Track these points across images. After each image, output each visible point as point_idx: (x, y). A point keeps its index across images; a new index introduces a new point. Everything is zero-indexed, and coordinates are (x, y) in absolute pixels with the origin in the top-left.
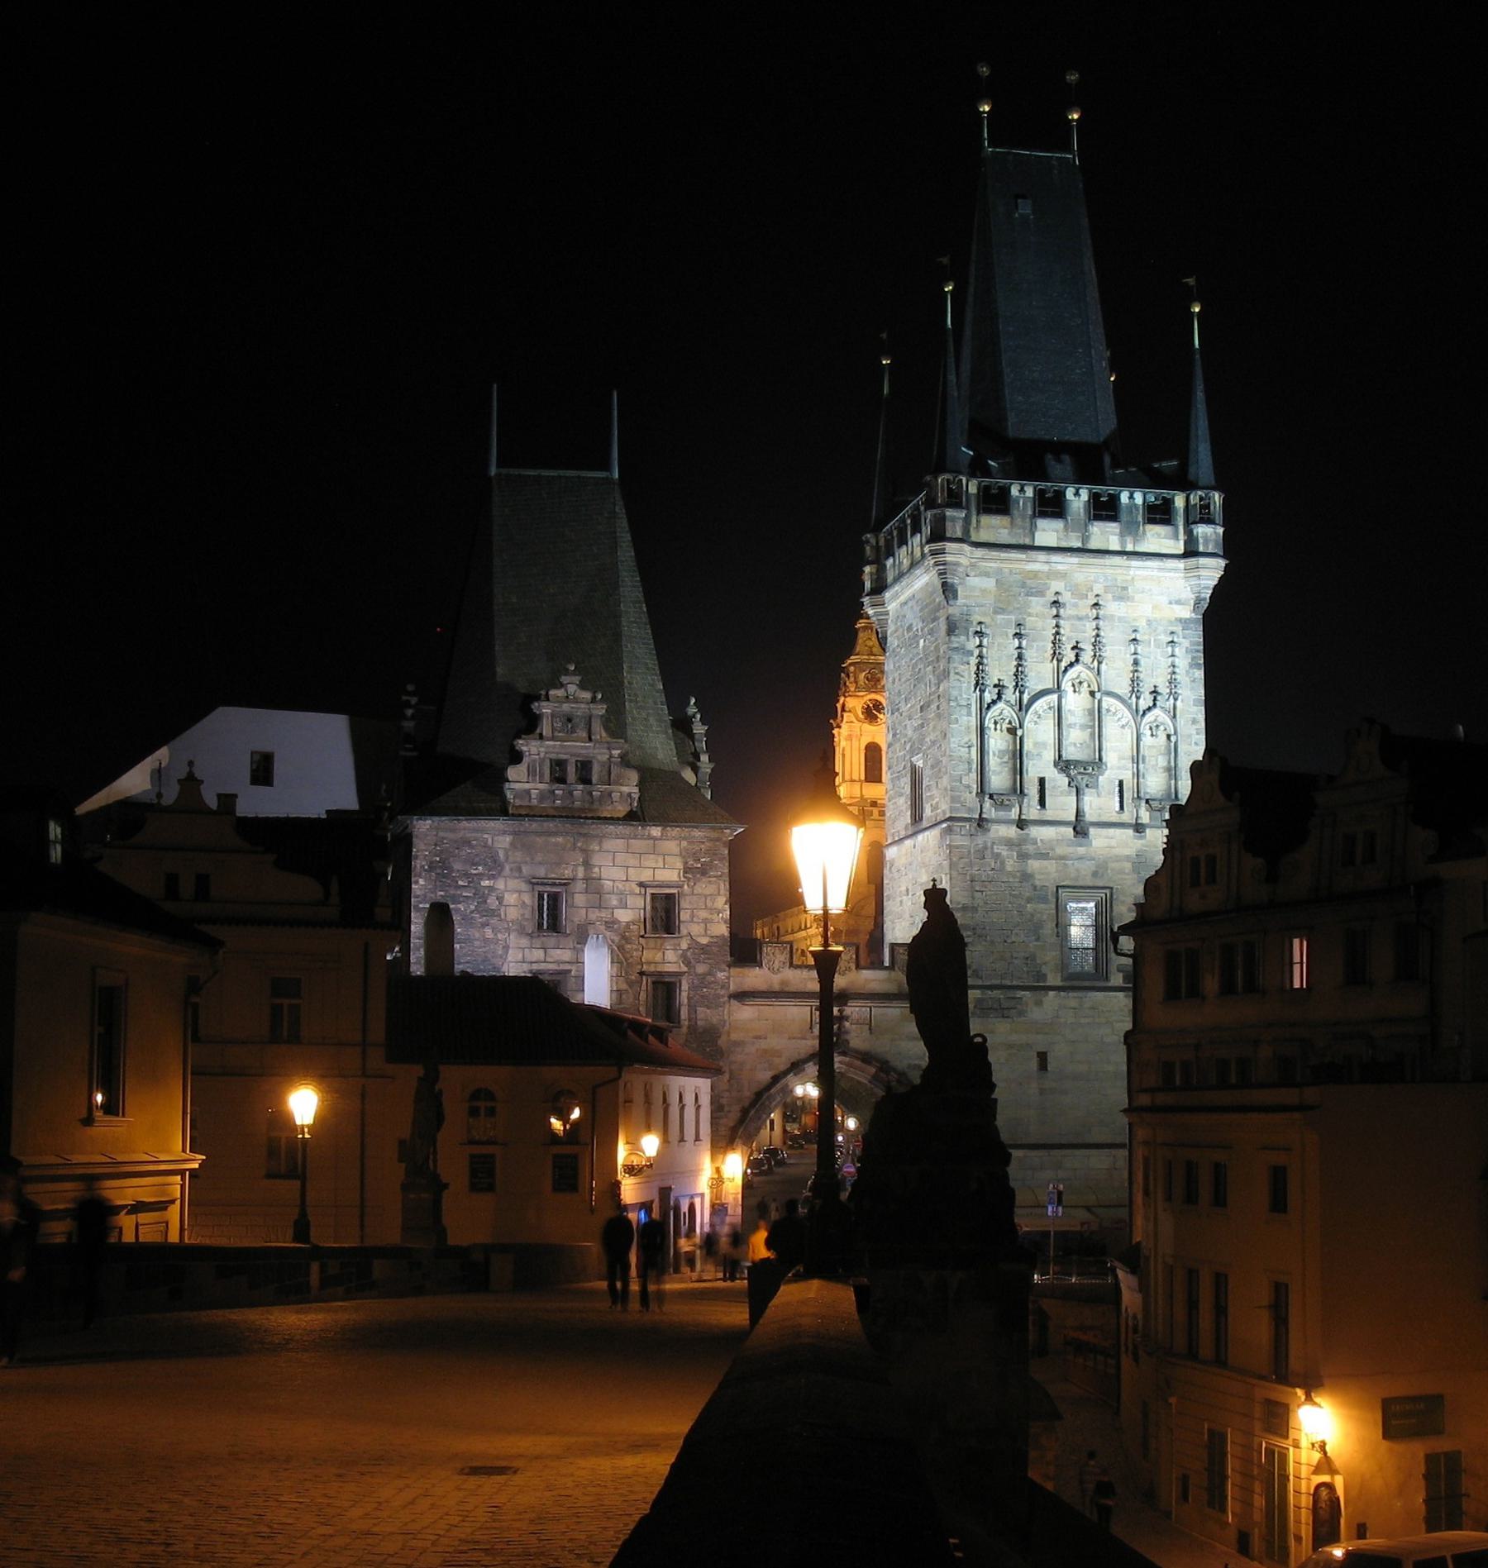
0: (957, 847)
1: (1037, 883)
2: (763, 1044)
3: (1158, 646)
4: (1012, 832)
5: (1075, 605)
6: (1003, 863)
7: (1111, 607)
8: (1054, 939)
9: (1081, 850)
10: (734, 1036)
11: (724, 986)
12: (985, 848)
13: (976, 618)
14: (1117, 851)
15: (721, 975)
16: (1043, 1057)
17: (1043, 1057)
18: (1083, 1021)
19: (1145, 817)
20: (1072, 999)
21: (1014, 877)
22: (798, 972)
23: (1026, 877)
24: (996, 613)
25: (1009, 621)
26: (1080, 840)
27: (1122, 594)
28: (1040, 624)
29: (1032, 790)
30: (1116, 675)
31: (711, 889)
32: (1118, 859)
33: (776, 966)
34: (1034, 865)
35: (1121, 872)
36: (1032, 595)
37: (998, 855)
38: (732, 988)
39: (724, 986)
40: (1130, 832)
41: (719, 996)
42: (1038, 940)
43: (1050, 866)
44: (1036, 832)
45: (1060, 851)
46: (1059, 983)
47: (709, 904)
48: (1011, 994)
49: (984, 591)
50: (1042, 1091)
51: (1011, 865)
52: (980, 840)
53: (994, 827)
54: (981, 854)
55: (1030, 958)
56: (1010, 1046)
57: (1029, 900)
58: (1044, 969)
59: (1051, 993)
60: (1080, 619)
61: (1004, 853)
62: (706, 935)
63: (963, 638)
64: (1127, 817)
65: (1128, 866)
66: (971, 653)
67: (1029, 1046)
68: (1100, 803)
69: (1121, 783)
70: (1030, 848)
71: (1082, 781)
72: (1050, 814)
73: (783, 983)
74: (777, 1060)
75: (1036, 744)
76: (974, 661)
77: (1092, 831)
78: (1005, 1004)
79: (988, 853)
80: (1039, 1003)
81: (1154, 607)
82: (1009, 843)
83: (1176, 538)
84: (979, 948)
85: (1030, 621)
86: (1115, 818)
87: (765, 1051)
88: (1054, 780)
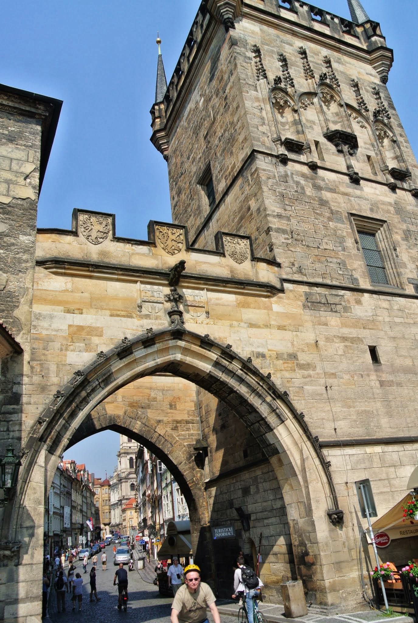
0: (264, 170)
1: (333, 208)
2: (78, 320)
3: (367, 91)
4: (305, 169)
5: (313, 57)
6: (303, 188)
7: (334, 65)
8: (355, 251)
9: (358, 192)
10: (37, 308)
11: (29, 250)
12: (286, 176)
13: (251, 41)
14: (382, 198)
15: (24, 239)
16: (373, 351)
17: (373, 351)
18: (397, 320)
19: (392, 180)
20: (383, 301)
21: (314, 200)
22: (121, 245)
23: (323, 203)
24: (263, 44)
25: (273, 50)
26: (354, 185)
27: (339, 61)
28: (293, 58)
29: (313, 148)
30: (348, 95)
31: (19, 154)
32: (383, 203)
33: (94, 234)
34: (327, 195)
35: (388, 212)
36: (284, 43)
37: (298, 183)
38: (40, 254)
39: (29, 250)
40: (386, 188)
41: (20, 261)
42: (344, 249)
43: (341, 199)
44: (320, 172)
45: (342, 189)
46: (369, 287)
47: (15, 167)
48: (334, 292)
49: (253, 32)
50: (382, 384)
51: (309, 191)
52: (281, 168)
53: (290, 163)
54: (285, 178)
55: (342, 264)
56: (344, 339)
57: (330, 219)
58: (356, 275)
59: (366, 295)
60: (318, 64)
61: (303, 182)
62: (8, 195)
63: (243, 49)
64: (379, 178)
65: (392, 209)
66: (250, 59)
67: (359, 340)
68: (360, 167)
69: (369, 157)
70: (322, 184)
71: (346, 148)
72: (328, 165)
73: (103, 253)
74: (95, 340)
75: (307, 120)
76: (253, 63)
77: (362, 182)
78: (331, 300)
79: (289, 179)
80: (359, 302)
81: (359, 73)
82: (303, 175)
83: (361, 43)
84: (298, 249)
85: (287, 55)
86: (372, 177)
87: (81, 328)
88: (326, 145)
